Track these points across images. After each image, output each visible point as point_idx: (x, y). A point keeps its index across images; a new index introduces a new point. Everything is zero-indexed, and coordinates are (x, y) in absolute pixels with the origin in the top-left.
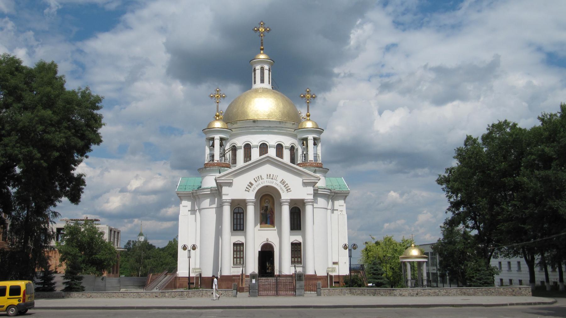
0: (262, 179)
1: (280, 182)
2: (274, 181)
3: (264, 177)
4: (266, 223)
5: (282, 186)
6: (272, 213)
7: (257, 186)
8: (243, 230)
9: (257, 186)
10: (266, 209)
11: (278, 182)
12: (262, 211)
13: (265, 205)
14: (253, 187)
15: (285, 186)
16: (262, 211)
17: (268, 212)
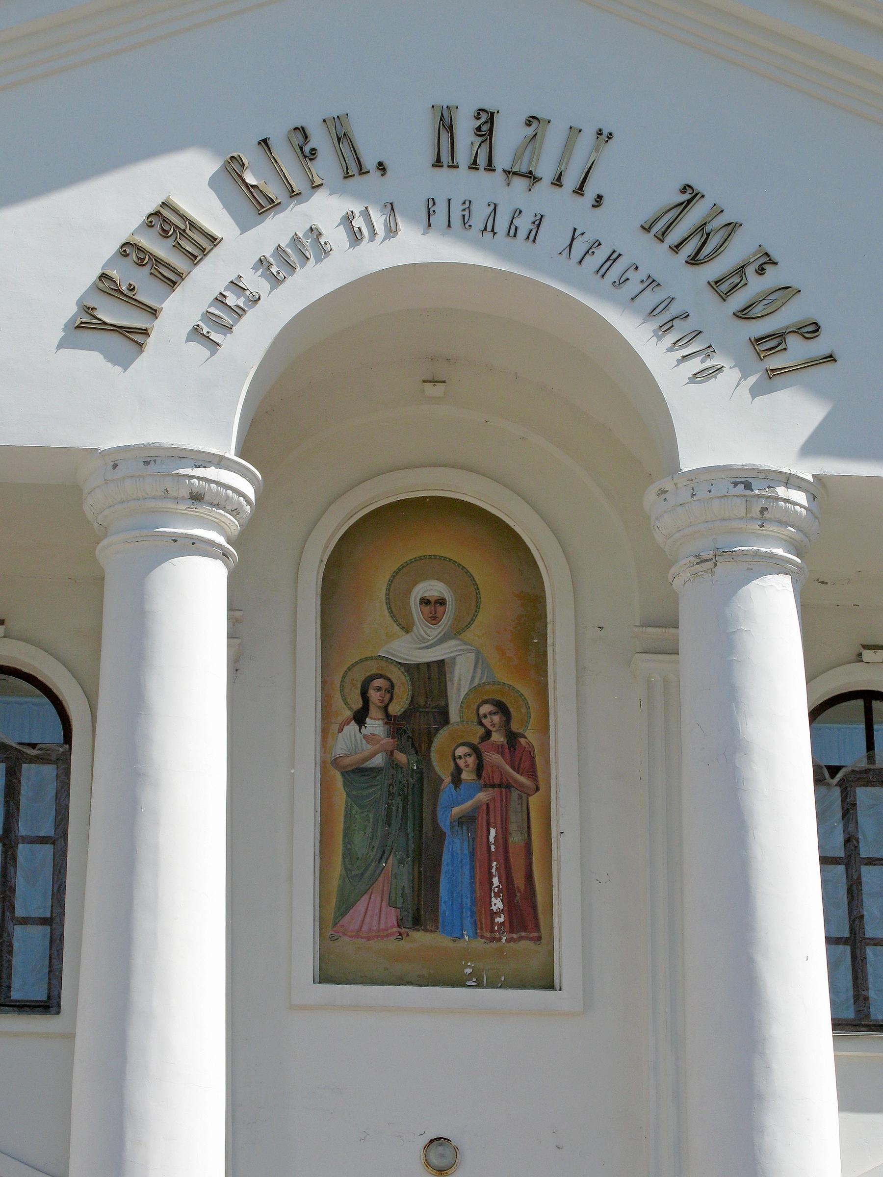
0: (354, 168)
1: (657, 228)
2: (560, 209)
3: (398, 135)
4: (420, 911)
5: (689, 285)
6: (514, 758)
7: (278, 266)
8: (48, 1005)
9: (278, 266)
10: (418, 709)
11: (618, 227)
12: (350, 740)
13: (410, 649)
14: (206, 280)
15: (723, 288)
16: (350, 740)
17: (447, 750)
